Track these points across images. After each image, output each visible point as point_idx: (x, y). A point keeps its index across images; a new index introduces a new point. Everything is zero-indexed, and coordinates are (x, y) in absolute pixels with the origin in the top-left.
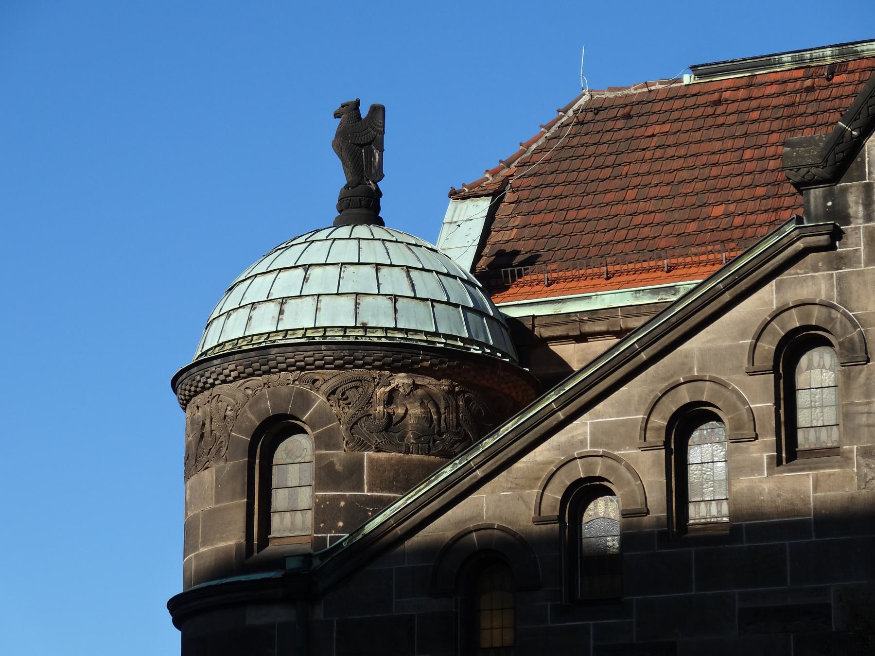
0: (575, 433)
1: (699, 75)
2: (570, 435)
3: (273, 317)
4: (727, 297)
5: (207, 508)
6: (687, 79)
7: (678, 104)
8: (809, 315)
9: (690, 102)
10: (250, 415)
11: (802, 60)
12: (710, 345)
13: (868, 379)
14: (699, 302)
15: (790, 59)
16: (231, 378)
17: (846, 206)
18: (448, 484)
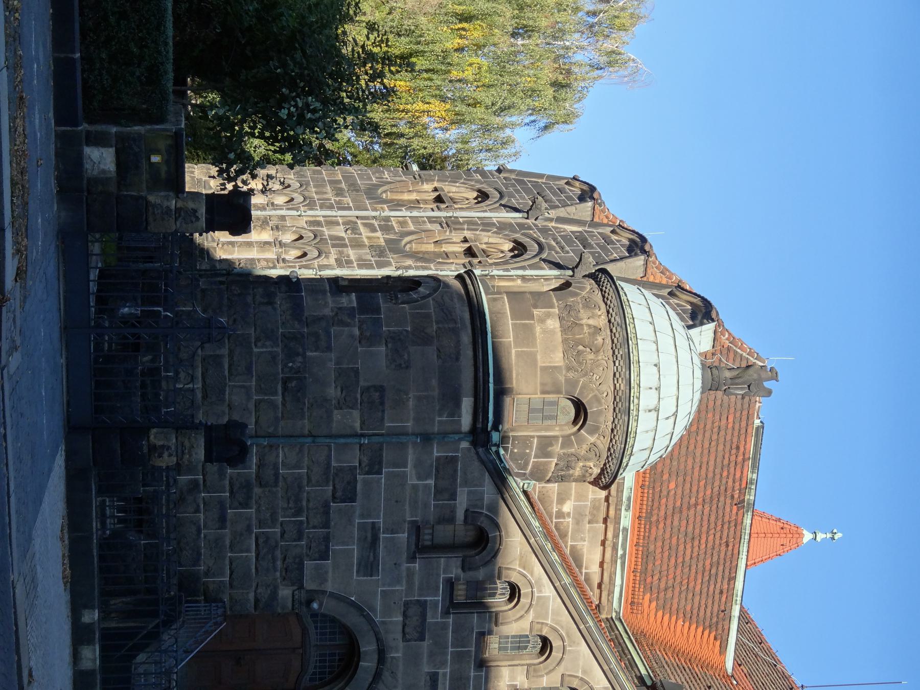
0: (546, 587)
1: (758, 428)
2: (546, 585)
3: (648, 406)
4: (606, 668)
5: (539, 357)
6: (757, 422)
7: (744, 424)
9: (743, 431)
10: (591, 395)
11: (751, 483)
12: (582, 655)
14: (605, 656)
15: (753, 478)
16: (616, 382)
18: (529, 525)
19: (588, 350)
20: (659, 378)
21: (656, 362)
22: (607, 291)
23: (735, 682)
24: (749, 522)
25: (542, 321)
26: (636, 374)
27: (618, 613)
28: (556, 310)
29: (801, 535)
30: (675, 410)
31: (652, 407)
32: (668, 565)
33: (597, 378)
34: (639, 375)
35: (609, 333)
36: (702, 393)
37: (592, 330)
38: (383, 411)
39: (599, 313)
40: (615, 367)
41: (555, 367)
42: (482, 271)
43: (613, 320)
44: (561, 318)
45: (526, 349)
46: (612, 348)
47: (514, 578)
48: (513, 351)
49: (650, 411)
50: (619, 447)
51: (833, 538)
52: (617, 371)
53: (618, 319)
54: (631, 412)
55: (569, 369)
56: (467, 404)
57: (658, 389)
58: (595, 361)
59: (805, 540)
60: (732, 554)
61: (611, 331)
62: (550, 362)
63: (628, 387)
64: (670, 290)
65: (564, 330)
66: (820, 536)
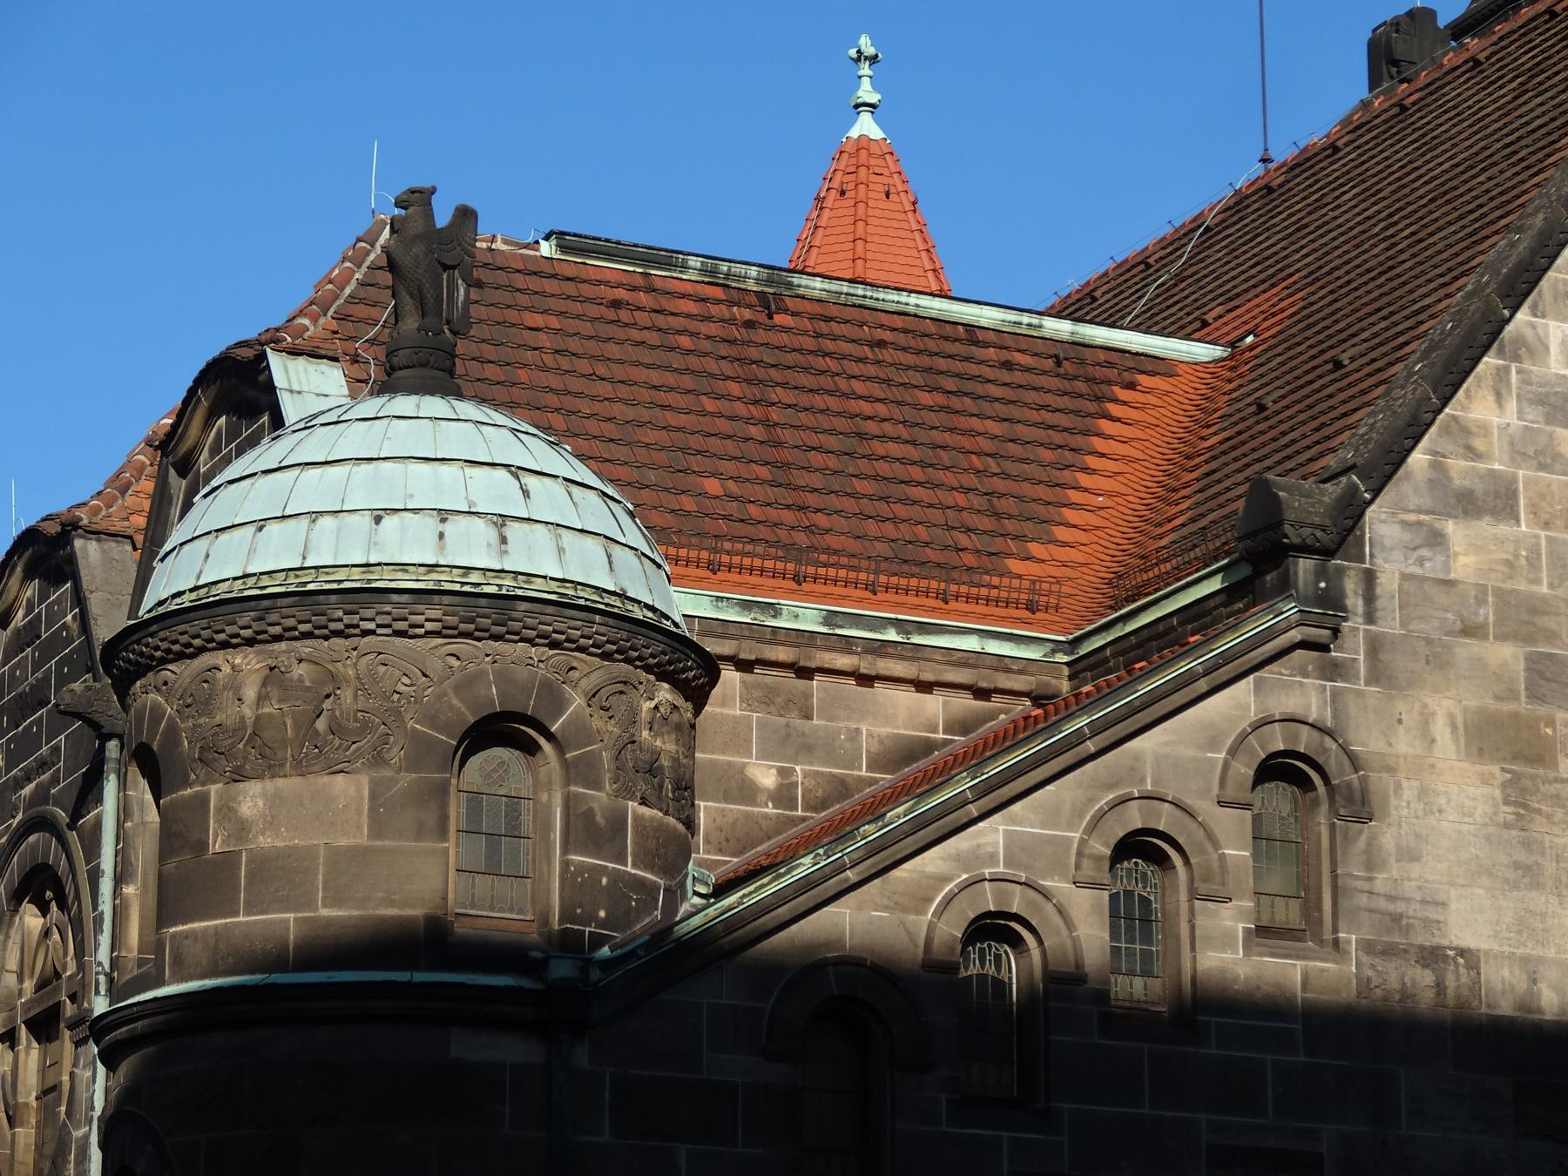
0: (981, 841)
1: (562, 248)
2: (974, 842)
3: (489, 545)
4: (1202, 685)
5: (344, 842)
6: (546, 249)
7: (550, 286)
8: (1296, 737)
9: (570, 288)
10: (455, 702)
11: (714, 272)
12: (1168, 749)
13: (1369, 844)
14: (1171, 686)
15: (698, 265)
16: (421, 631)
17: (1342, 595)
18: (807, 884)
19: (327, 704)
20: (415, 511)
21: (367, 519)
22: (164, 645)
23: (1250, 339)
24: (818, 283)
25: (242, 829)
26: (400, 575)
27: (1058, 647)
28: (214, 789)
29: (864, 143)
30: (502, 474)
31: (491, 534)
32: (931, 506)
33: (406, 680)
34: (403, 566)
35: (283, 645)
36: (460, 395)
37: (275, 694)
39: (226, 669)
40: (380, 631)
41: (373, 797)
42: (97, 993)
43: (247, 633)
44: (239, 776)
45: (321, 877)
46: (326, 638)
47: (953, 928)
48: (325, 912)
49: (504, 540)
50: (598, 626)
51: (873, 60)
52: (389, 626)
53: (246, 619)
54: (504, 592)
55: (379, 760)
56: (469, 1047)
57: (443, 515)
58: (361, 687)
59: (876, 133)
60: (906, 331)
61: (277, 638)
62: (359, 812)
63: (436, 598)
64: (172, 472)
65: (270, 767)
66: (867, 93)
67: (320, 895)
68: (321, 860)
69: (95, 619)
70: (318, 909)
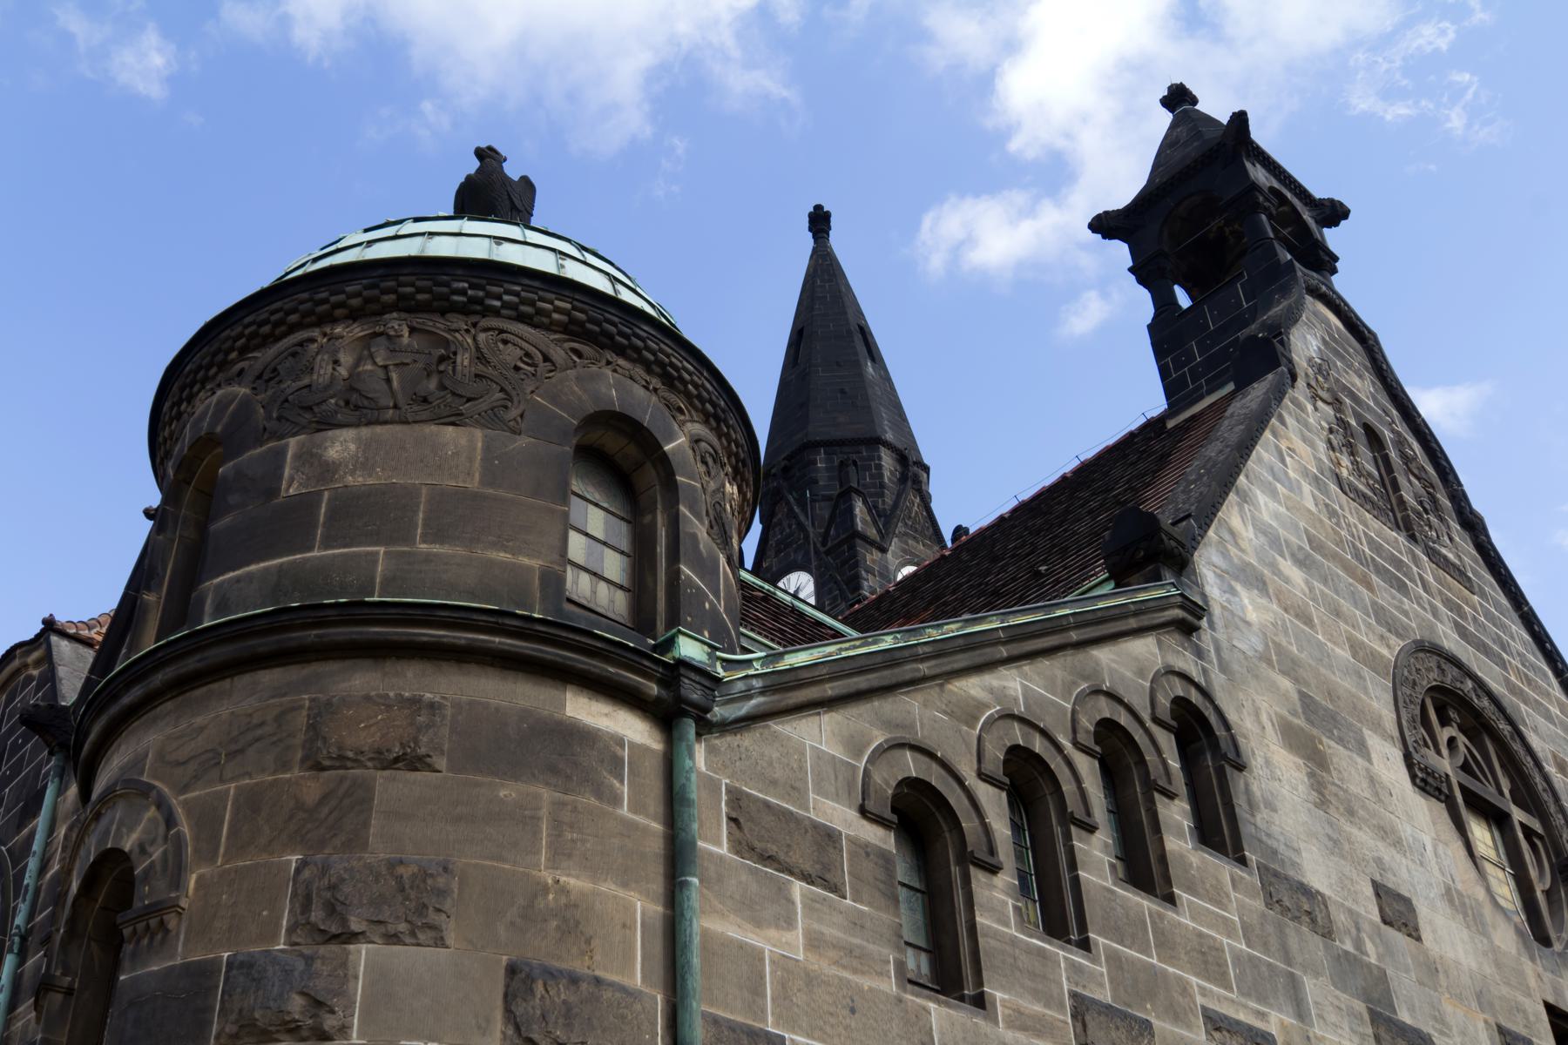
10: (576, 389)
25: (328, 471)
28: (293, 443)
38: (598, 981)
41: (487, 448)
42: (24, 900)
43: (355, 302)
45: (421, 515)
46: (443, 313)
62: (471, 460)
67: (419, 531)
68: (423, 500)
69: (61, 680)
70: (415, 543)
